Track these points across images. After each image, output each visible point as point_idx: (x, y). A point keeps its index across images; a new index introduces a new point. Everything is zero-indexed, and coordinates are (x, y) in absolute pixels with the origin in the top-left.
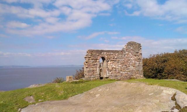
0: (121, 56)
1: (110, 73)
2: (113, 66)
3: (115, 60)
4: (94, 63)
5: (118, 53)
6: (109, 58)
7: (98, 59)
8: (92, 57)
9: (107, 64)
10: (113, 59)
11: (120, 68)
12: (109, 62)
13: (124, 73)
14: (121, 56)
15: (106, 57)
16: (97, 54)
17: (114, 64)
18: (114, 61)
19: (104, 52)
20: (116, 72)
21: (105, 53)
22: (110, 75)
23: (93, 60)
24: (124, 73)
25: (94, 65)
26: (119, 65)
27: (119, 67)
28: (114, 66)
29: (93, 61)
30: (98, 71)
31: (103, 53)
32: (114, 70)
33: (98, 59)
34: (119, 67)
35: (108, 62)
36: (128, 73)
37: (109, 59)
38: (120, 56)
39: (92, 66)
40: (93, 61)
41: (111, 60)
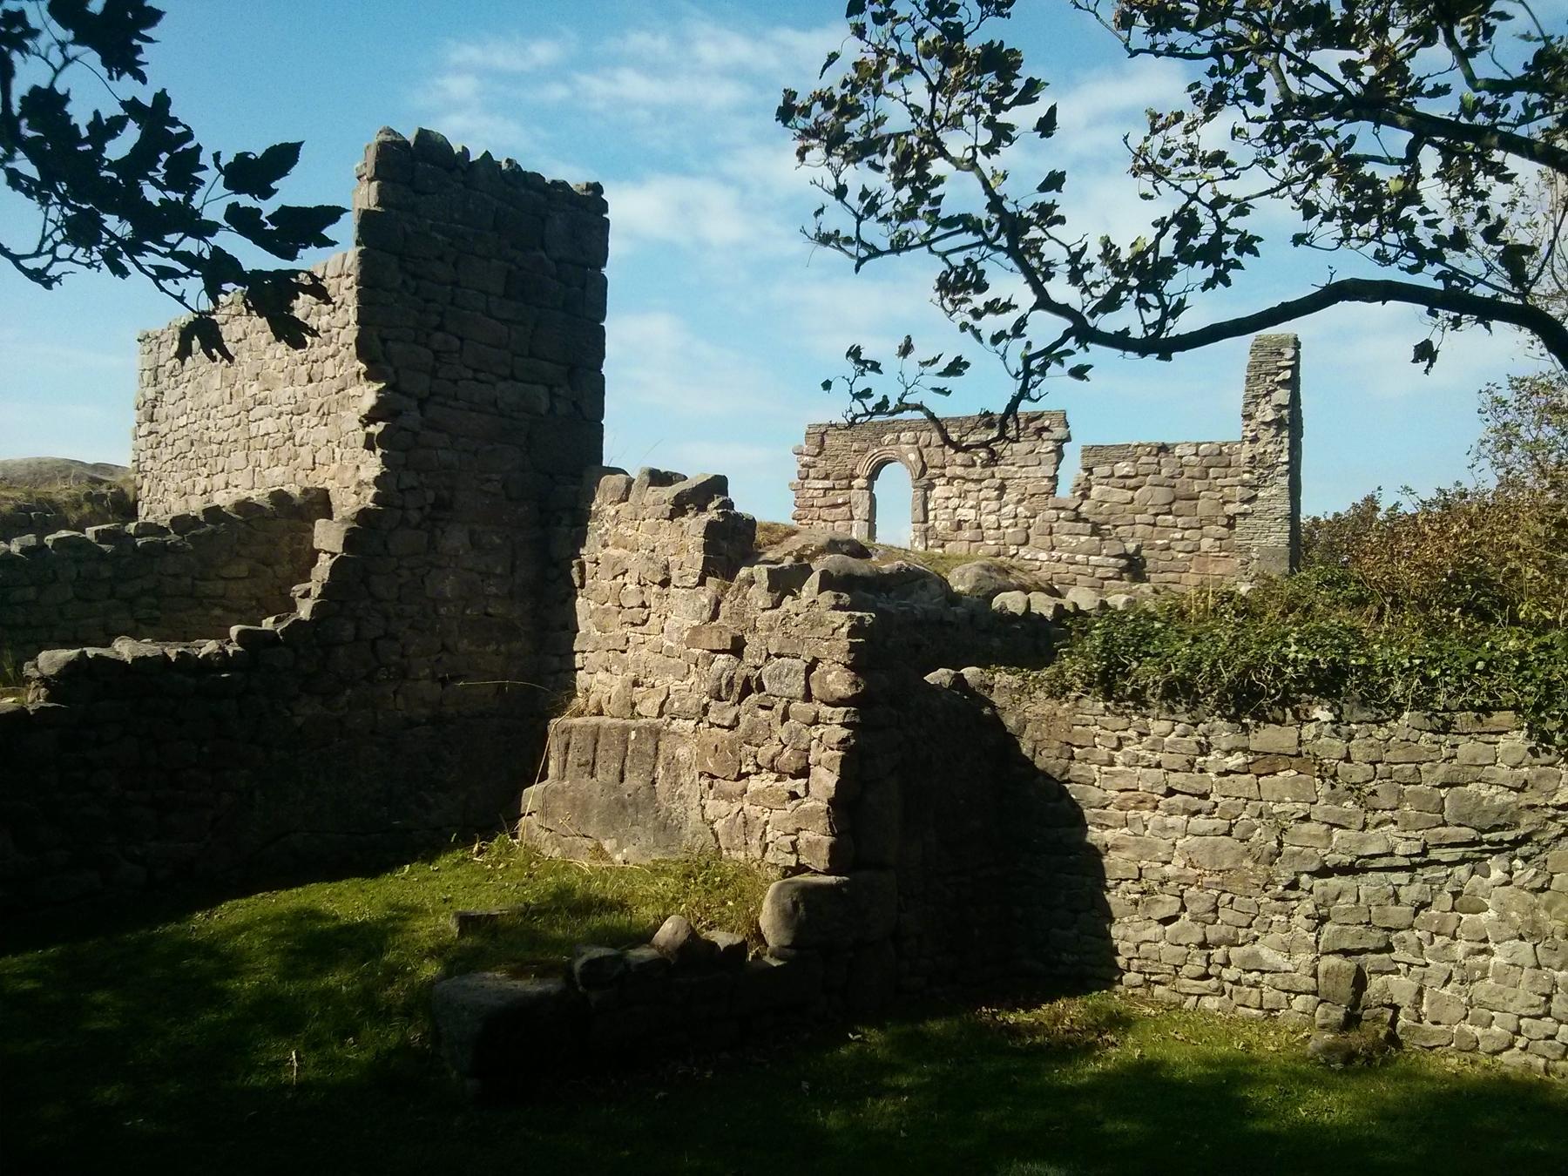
4: (832, 498)
7: (858, 471)
8: (821, 464)
9: (920, 502)
10: (959, 471)
12: (939, 492)
16: (855, 446)
17: (971, 503)
18: (973, 480)
21: (907, 436)
29: (827, 483)
31: (888, 437)
33: (858, 471)
35: (931, 486)
36: (1079, 558)
37: (937, 471)
39: (825, 513)
40: (827, 483)
41: (954, 478)
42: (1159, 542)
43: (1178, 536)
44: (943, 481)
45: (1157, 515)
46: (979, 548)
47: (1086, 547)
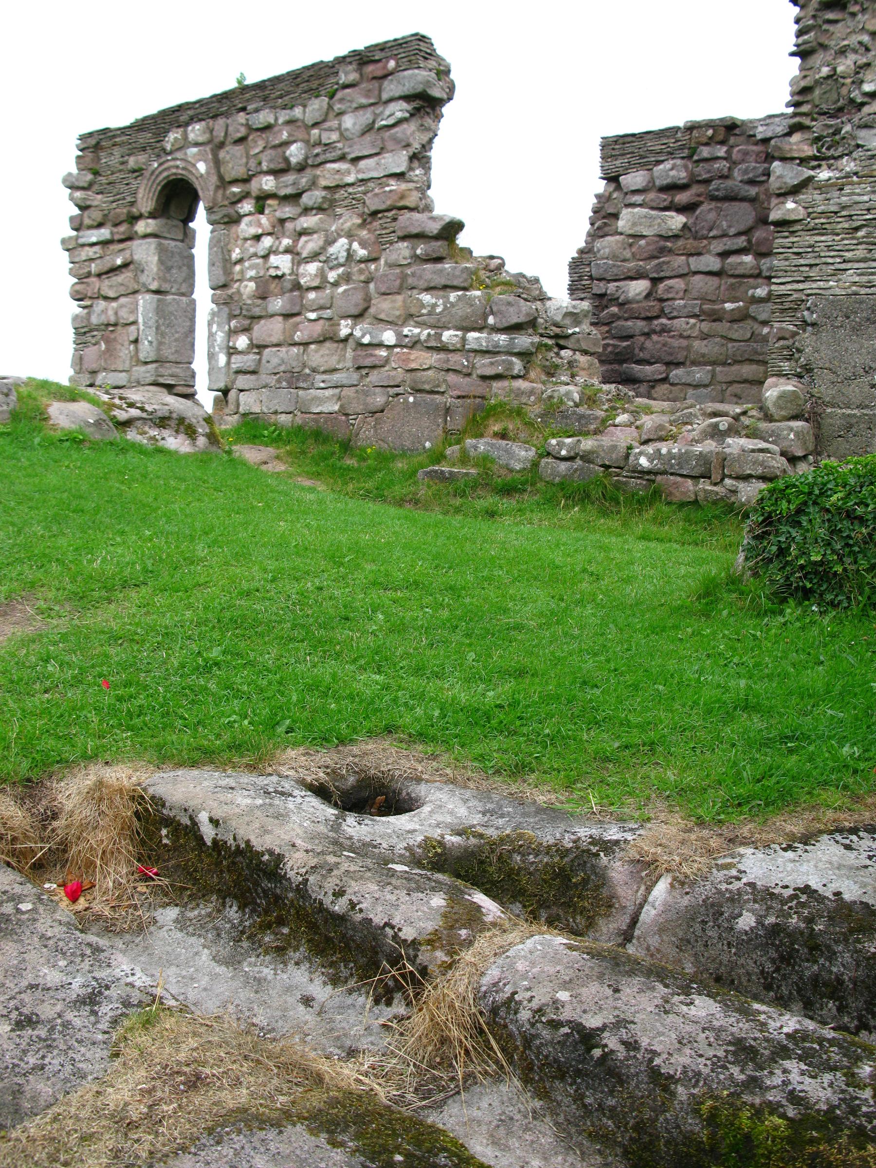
0: (366, 117)
1: (242, 342)
2: (274, 260)
3: (288, 183)
5: (315, 93)
6: (239, 171)
10: (268, 183)
11: (346, 278)
12: (246, 228)
13: (389, 337)
14: (366, 117)
15: (202, 167)
19: (192, 120)
20: (298, 336)
21: (196, 131)
22: (238, 362)
23: (100, 225)
24: (389, 337)
25: (114, 270)
26: (339, 247)
27: (330, 263)
28: (282, 263)
29: (105, 233)
30: (142, 328)
31: (173, 136)
32: (277, 304)
34: (330, 263)
36: (448, 336)
38: (348, 122)
40: (105, 233)
42: (728, 306)
43: (761, 292)
44: (247, 206)
45: (724, 255)
46: (296, 327)
47: (461, 311)
